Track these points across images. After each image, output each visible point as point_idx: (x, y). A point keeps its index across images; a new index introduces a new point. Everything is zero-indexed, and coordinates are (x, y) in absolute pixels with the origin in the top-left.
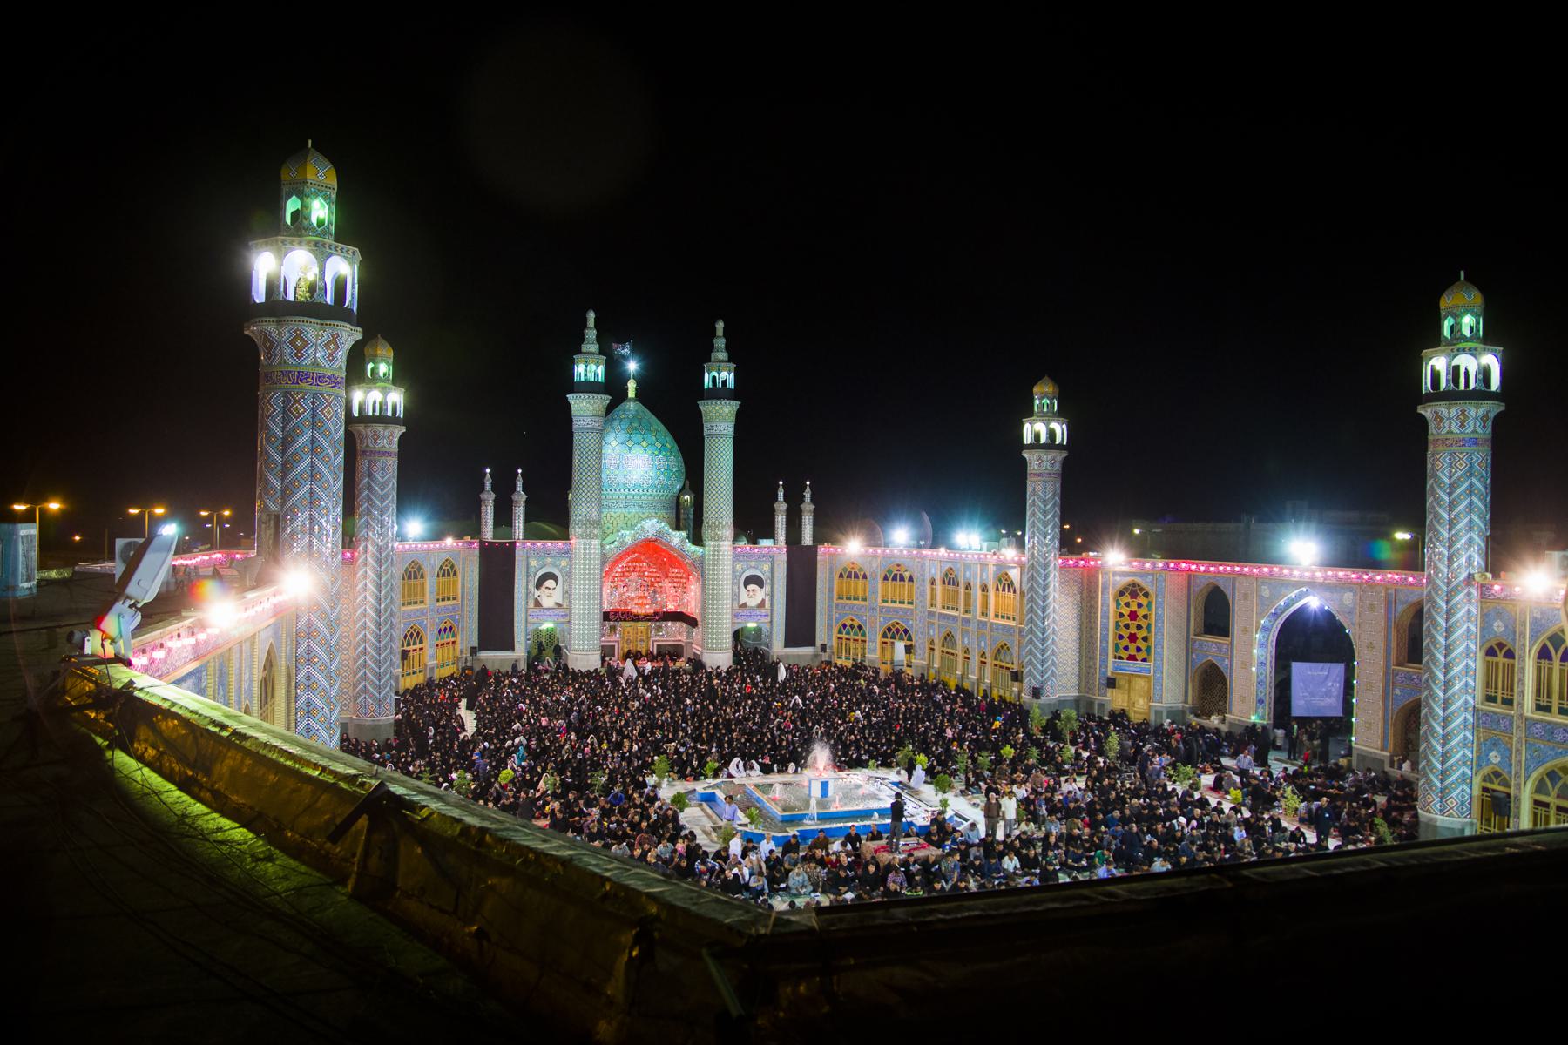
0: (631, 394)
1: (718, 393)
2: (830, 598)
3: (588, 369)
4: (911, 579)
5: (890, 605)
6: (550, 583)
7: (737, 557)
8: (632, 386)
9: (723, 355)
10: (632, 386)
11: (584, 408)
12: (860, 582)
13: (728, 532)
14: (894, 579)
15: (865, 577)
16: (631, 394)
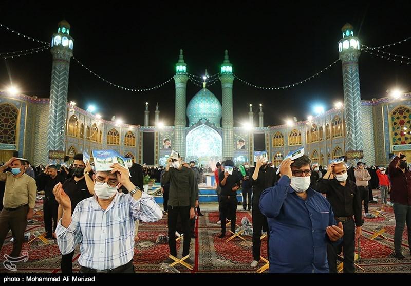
0: (204, 86)
1: (224, 74)
2: (271, 147)
3: (181, 68)
4: (300, 134)
5: (292, 145)
6: (167, 141)
7: (235, 131)
8: (204, 84)
9: (227, 61)
10: (204, 84)
11: (180, 84)
12: (281, 138)
13: (232, 123)
14: (294, 135)
15: (283, 136)
16: (204, 86)
